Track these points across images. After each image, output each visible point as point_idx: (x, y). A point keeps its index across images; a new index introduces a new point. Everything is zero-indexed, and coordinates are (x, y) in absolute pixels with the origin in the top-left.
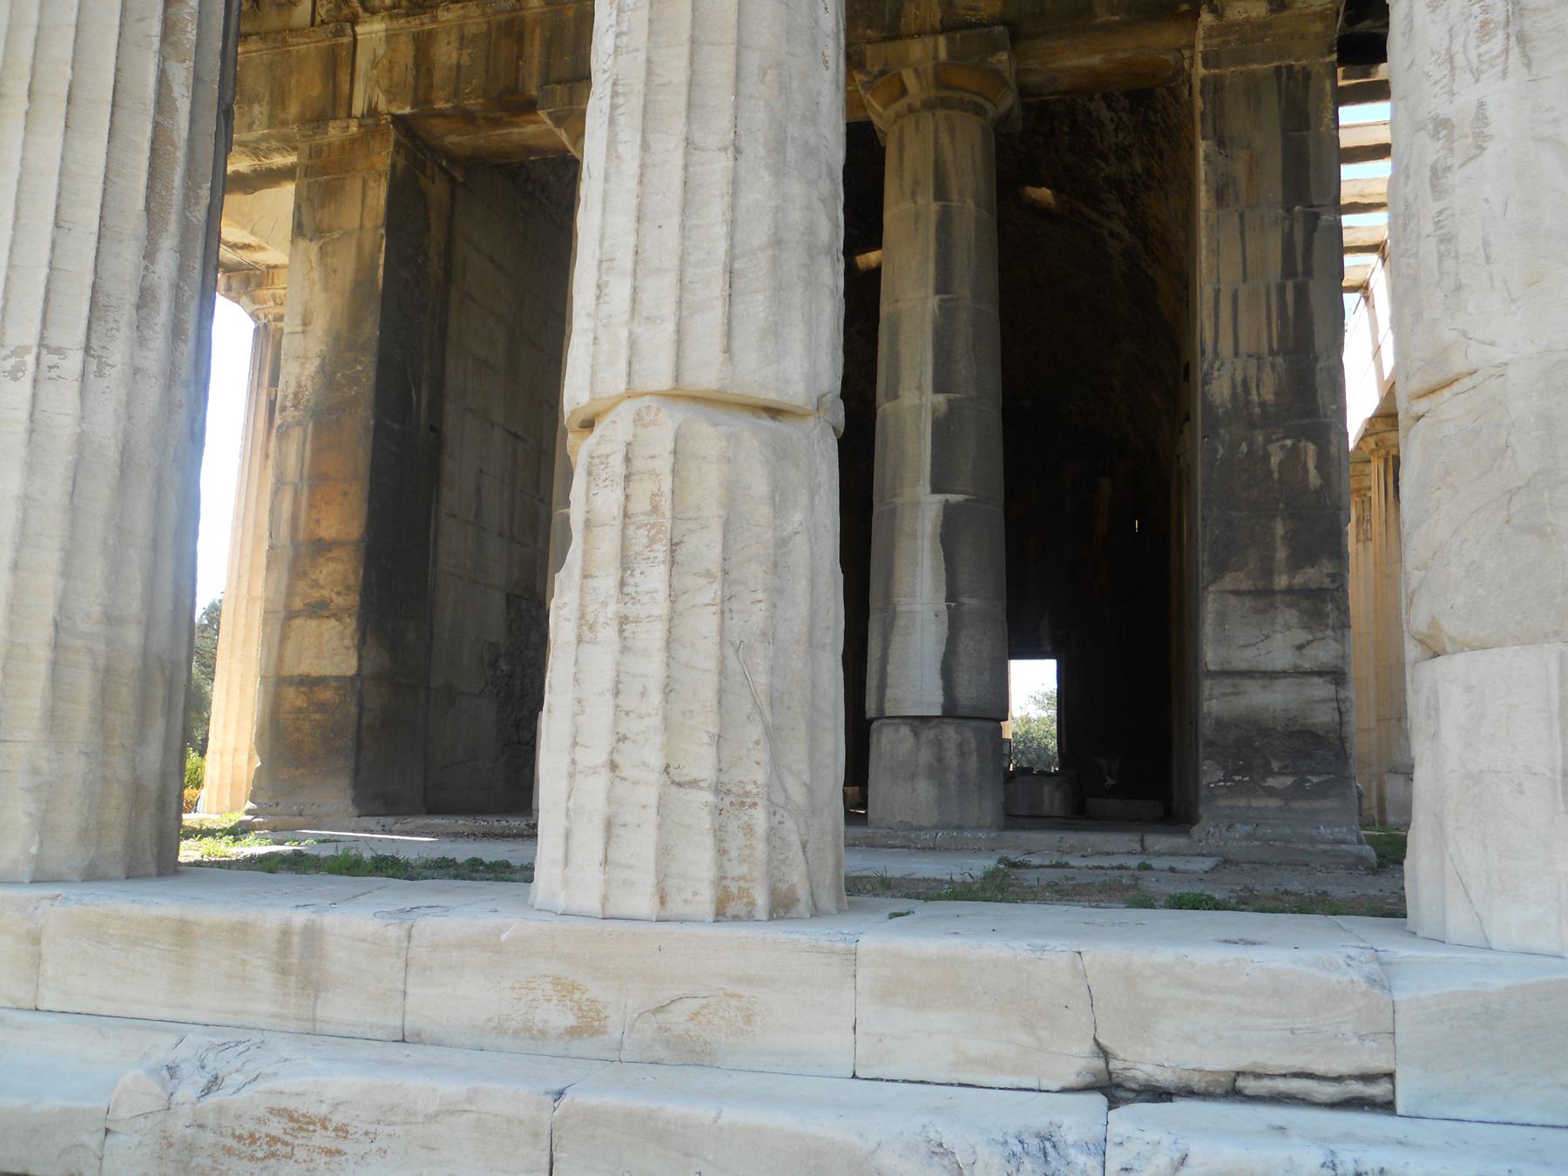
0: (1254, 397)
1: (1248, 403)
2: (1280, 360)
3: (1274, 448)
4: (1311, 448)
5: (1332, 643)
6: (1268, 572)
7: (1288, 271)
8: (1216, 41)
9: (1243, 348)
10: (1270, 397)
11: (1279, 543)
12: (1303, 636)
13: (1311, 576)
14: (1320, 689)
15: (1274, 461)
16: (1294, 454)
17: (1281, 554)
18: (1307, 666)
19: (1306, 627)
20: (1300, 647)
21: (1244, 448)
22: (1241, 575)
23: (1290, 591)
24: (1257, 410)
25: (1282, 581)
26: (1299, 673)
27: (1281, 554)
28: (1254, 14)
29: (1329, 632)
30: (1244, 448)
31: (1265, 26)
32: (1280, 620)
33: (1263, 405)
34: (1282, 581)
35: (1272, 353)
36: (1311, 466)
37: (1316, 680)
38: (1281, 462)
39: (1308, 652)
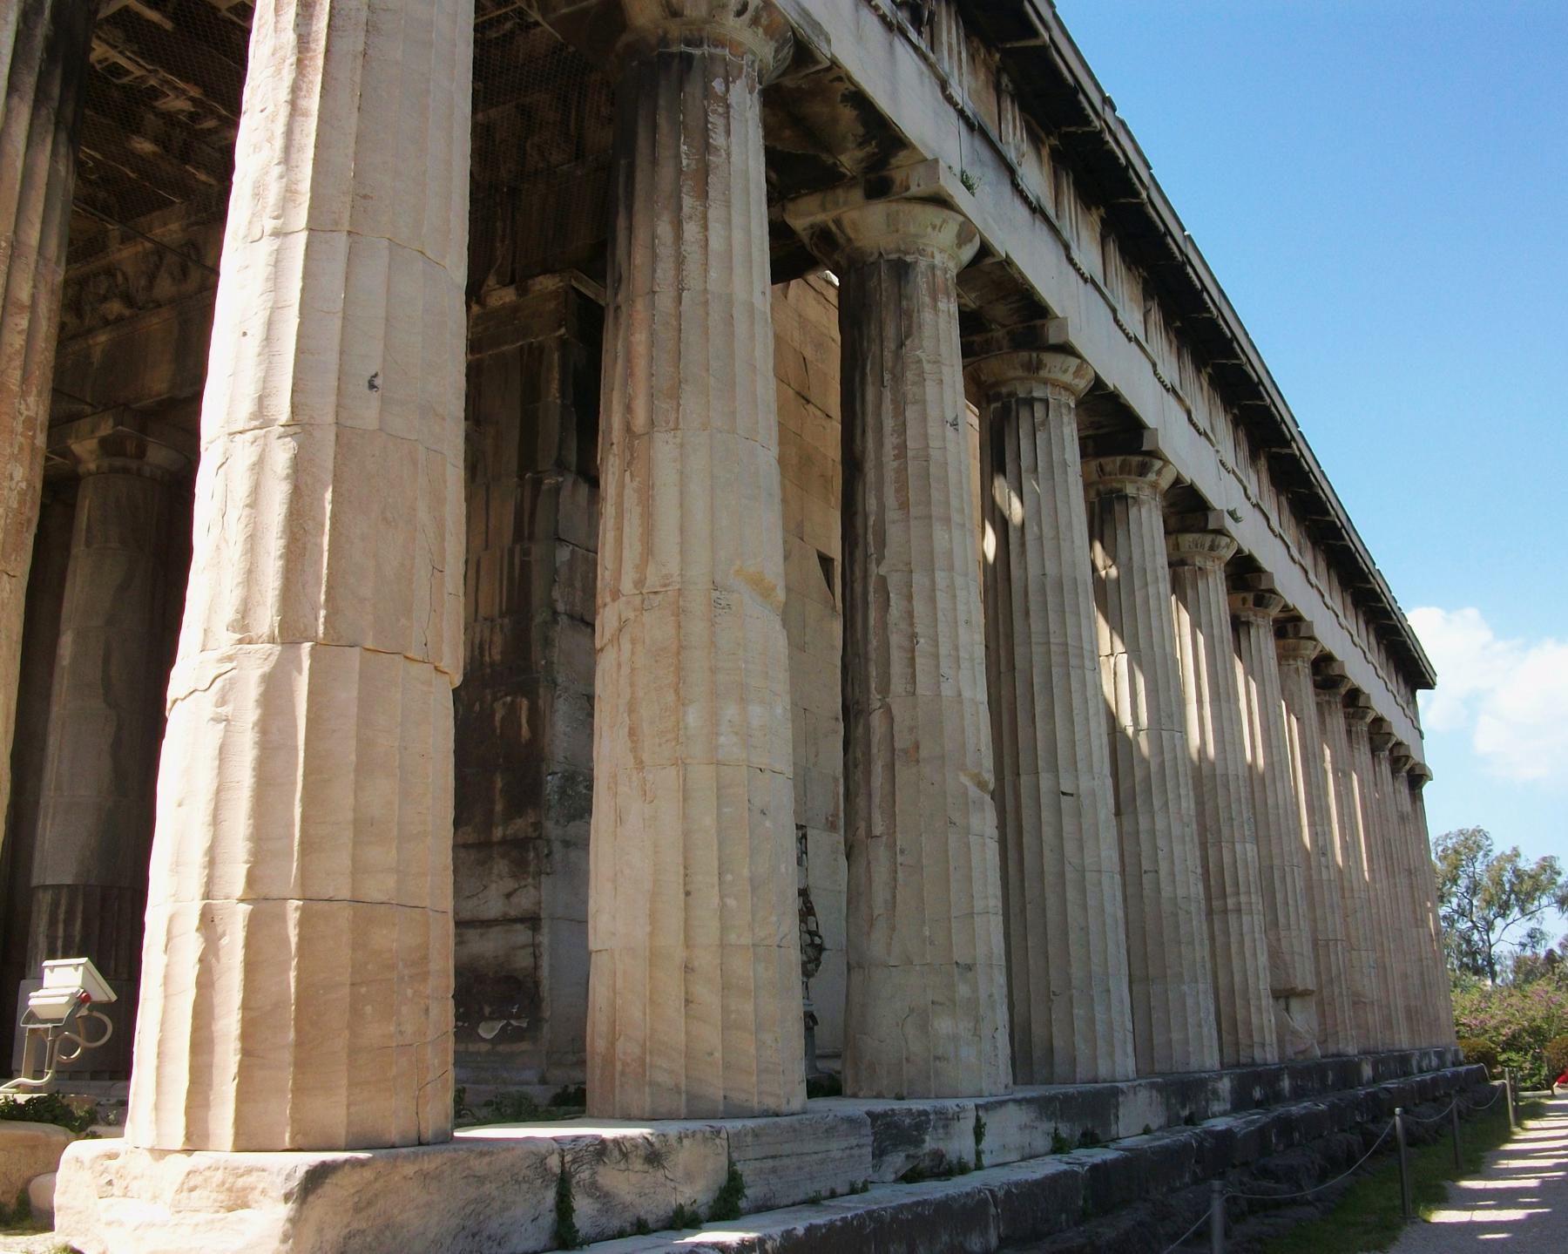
0: (487, 659)
1: (482, 664)
2: (506, 621)
3: (498, 706)
4: (525, 703)
5: (532, 890)
6: (489, 825)
7: (518, 535)
8: (480, 329)
9: (482, 612)
10: (497, 657)
11: (497, 797)
12: (510, 884)
13: (520, 826)
14: (522, 935)
15: (498, 717)
16: (512, 709)
17: (499, 807)
18: (513, 913)
19: (514, 876)
20: (509, 896)
21: (477, 707)
22: (469, 829)
23: (503, 841)
24: (488, 671)
25: (498, 833)
26: (507, 921)
27: (499, 807)
28: (507, 300)
29: (530, 880)
30: (477, 707)
31: (514, 310)
32: (495, 871)
33: (492, 664)
34: (498, 833)
35: (502, 615)
36: (524, 721)
37: (519, 927)
38: (503, 718)
39: (515, 900)
